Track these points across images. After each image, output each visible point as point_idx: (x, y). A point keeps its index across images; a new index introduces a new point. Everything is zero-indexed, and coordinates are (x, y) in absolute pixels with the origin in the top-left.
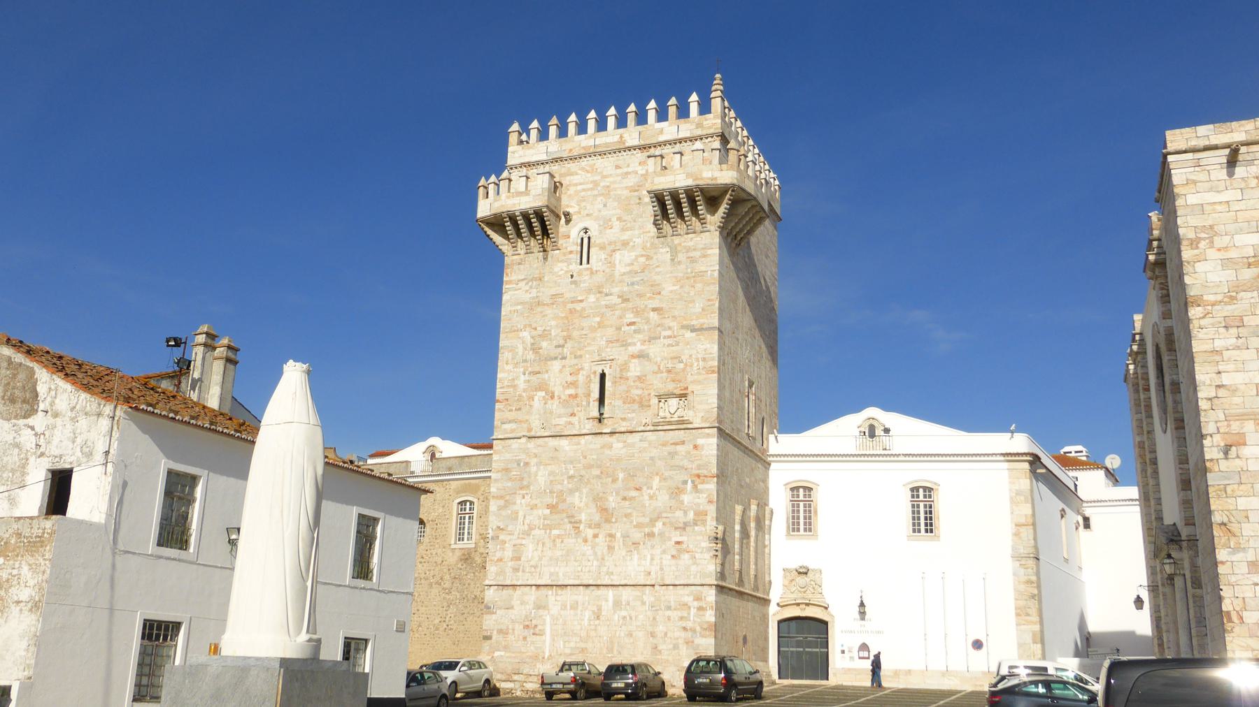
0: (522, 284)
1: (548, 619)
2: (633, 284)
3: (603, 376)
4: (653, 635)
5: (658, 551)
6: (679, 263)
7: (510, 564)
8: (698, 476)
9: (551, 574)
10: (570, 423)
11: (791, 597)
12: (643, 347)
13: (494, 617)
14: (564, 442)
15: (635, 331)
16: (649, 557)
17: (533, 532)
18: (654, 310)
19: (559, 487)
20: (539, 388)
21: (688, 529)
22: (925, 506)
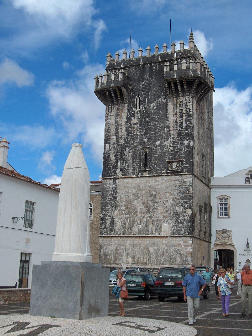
11: (219, 242)
14: (130, 180)
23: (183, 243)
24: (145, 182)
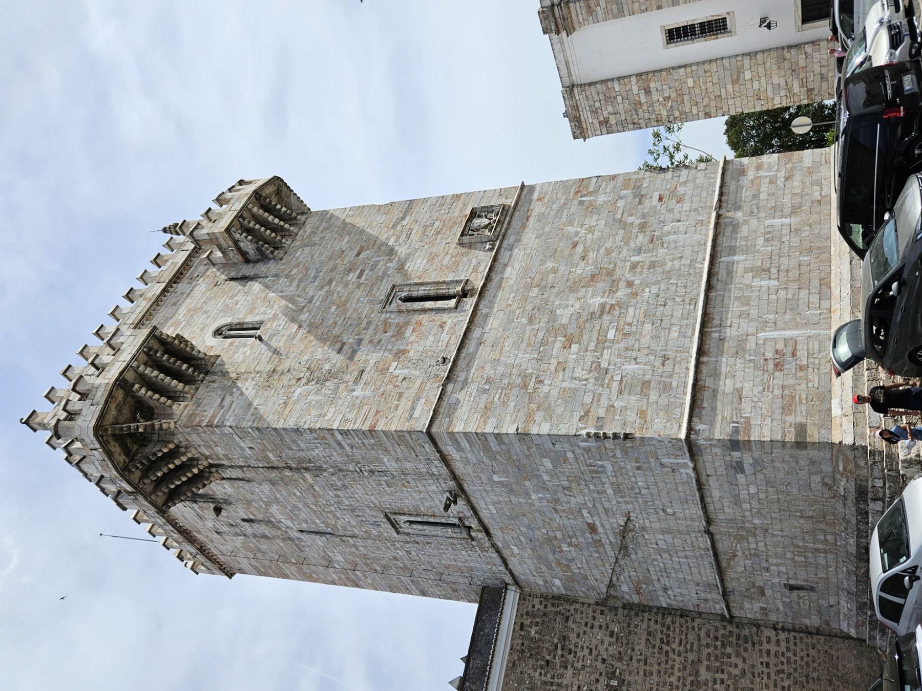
0: (226, 403)
6: (322, 238)
7: (653, 397)
9: (682, 335)
13: (756, 421)
17: (604, 365)
18: (358, 255)
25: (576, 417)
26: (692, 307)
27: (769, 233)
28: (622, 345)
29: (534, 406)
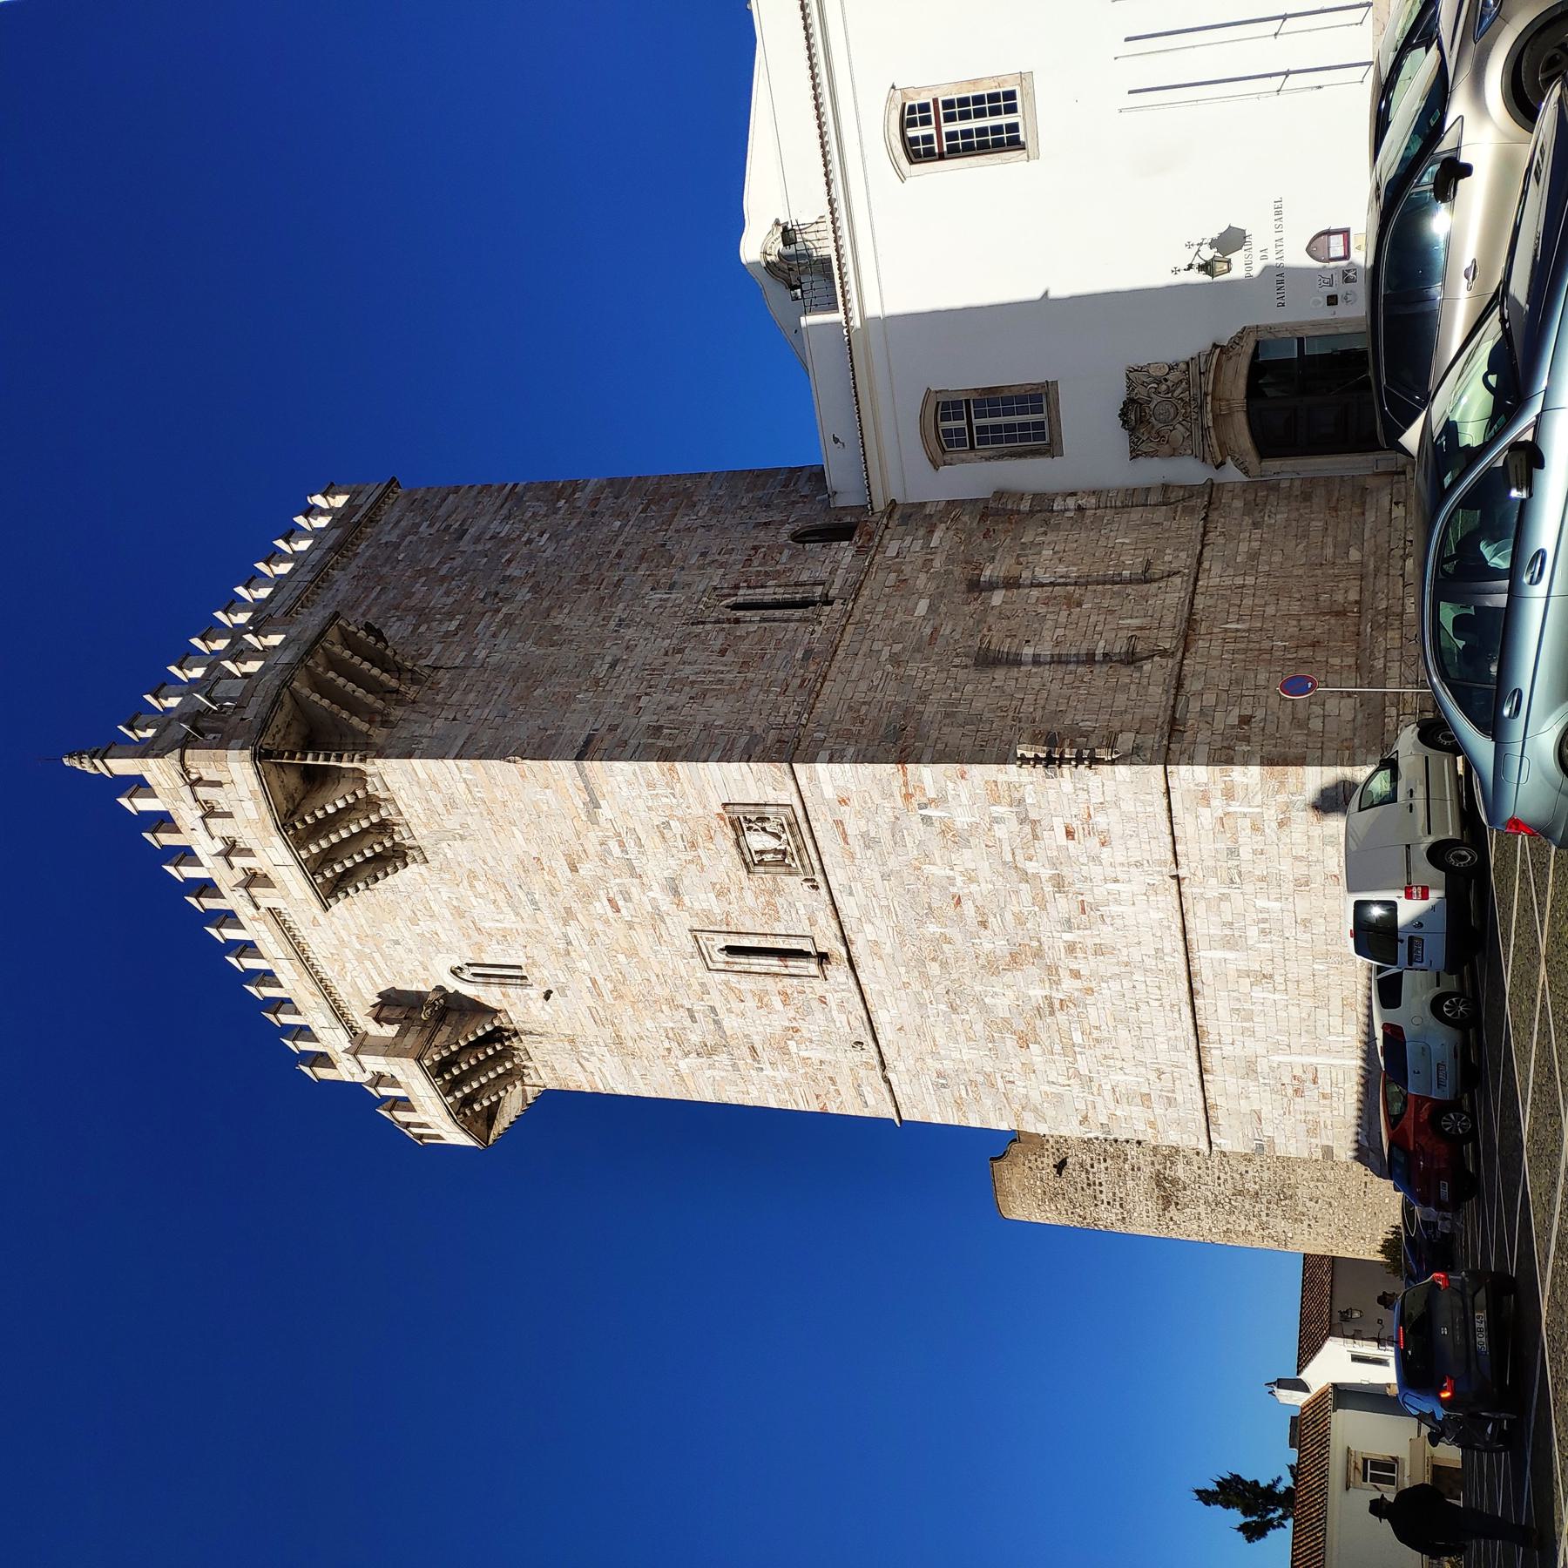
1: (1276, 1058)
2: (534, 902)
3: (732, 950)
4: (1303, 883)
5: (1096, 871)
8: (908, 796)
10: (841, 1004)
12: (655, 886)
14: (881, 1018)
15: (628, 899)
16: (1111, 886)
18: (574, 869)
19: (979, 1027)
20: (785, 1051)
21: (1033, 815)
22: (950, 118)
23: (1208, 806)
24: (878, 963)
25: (1075, 1122)
26: (1176, 1015)
27: (1265, 921)
28: (1099, 1052)
29: (1016, 1106)
